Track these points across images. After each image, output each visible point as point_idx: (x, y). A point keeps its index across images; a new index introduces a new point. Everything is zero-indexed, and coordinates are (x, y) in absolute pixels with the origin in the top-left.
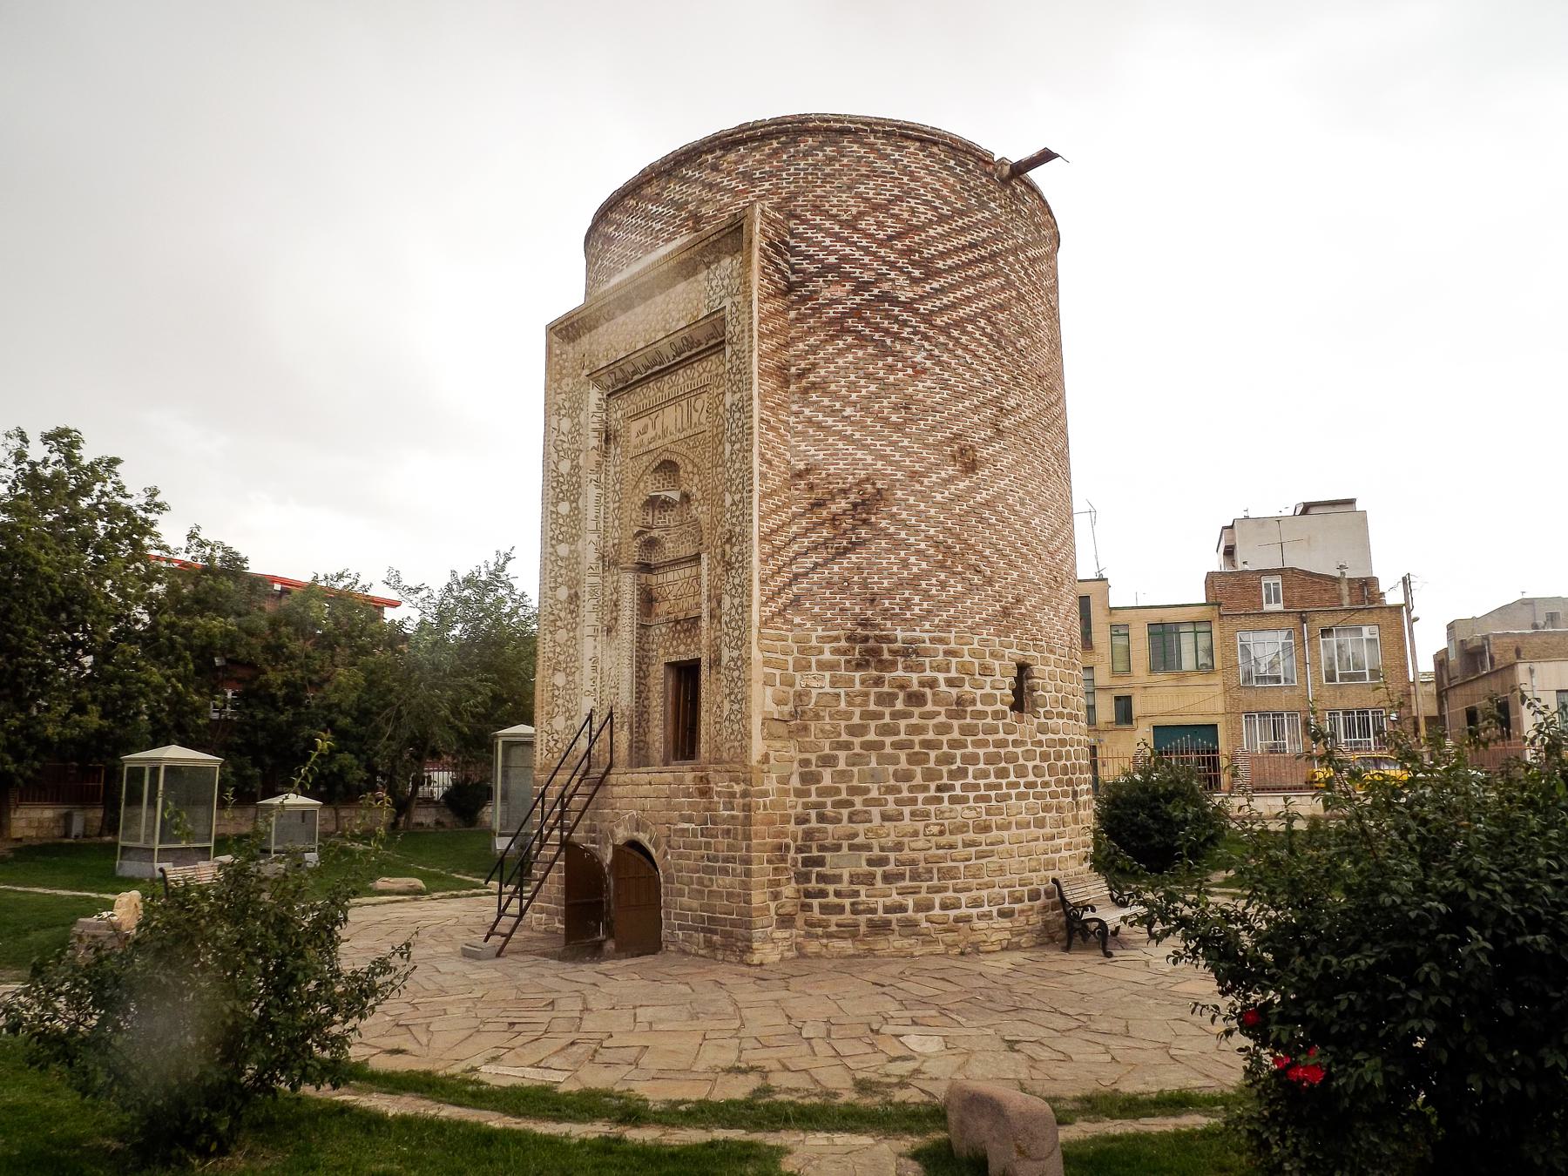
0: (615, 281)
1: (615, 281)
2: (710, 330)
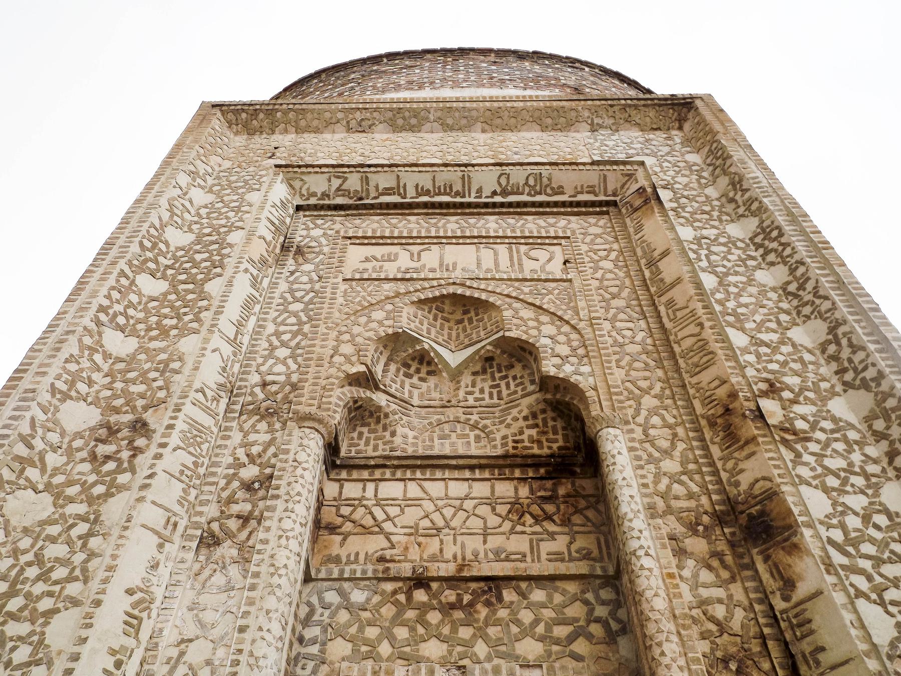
2: (592, 177)
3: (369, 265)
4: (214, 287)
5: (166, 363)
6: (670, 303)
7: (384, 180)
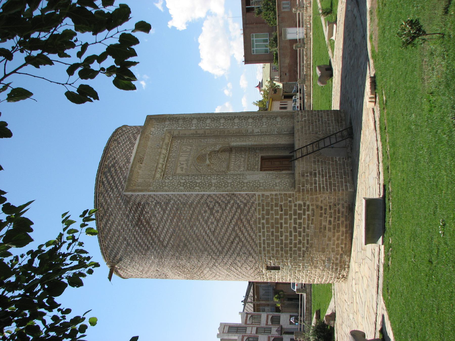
2: (167, 138)
3: (184, 171)
5: (218, 183)
6: (208, 134)
7: (160, 166)
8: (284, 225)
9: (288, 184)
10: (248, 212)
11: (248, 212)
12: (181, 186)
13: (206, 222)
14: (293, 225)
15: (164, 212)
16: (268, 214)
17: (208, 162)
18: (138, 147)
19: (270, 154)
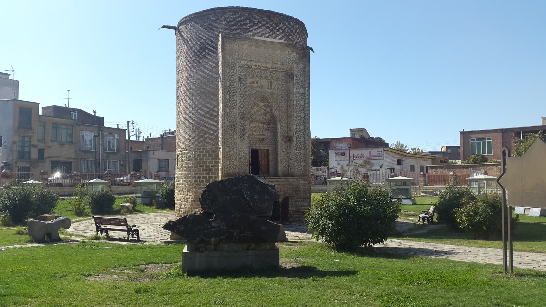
0: (256, 38)
1: (256, 38)
2: (285, 68)
3: (251, 85)
4: (235, 98)
7: (254, 64)
8: (202, 168)
9: (231, 171)
10: (211, 140)
11: (211, 140)
12: (230, 83)
13: (204, 106)
14: (202, 176)
15: (211, 70)
16: (210, 155)
17: (261, 104)
18: (271, 42)
19: (271, 157)
